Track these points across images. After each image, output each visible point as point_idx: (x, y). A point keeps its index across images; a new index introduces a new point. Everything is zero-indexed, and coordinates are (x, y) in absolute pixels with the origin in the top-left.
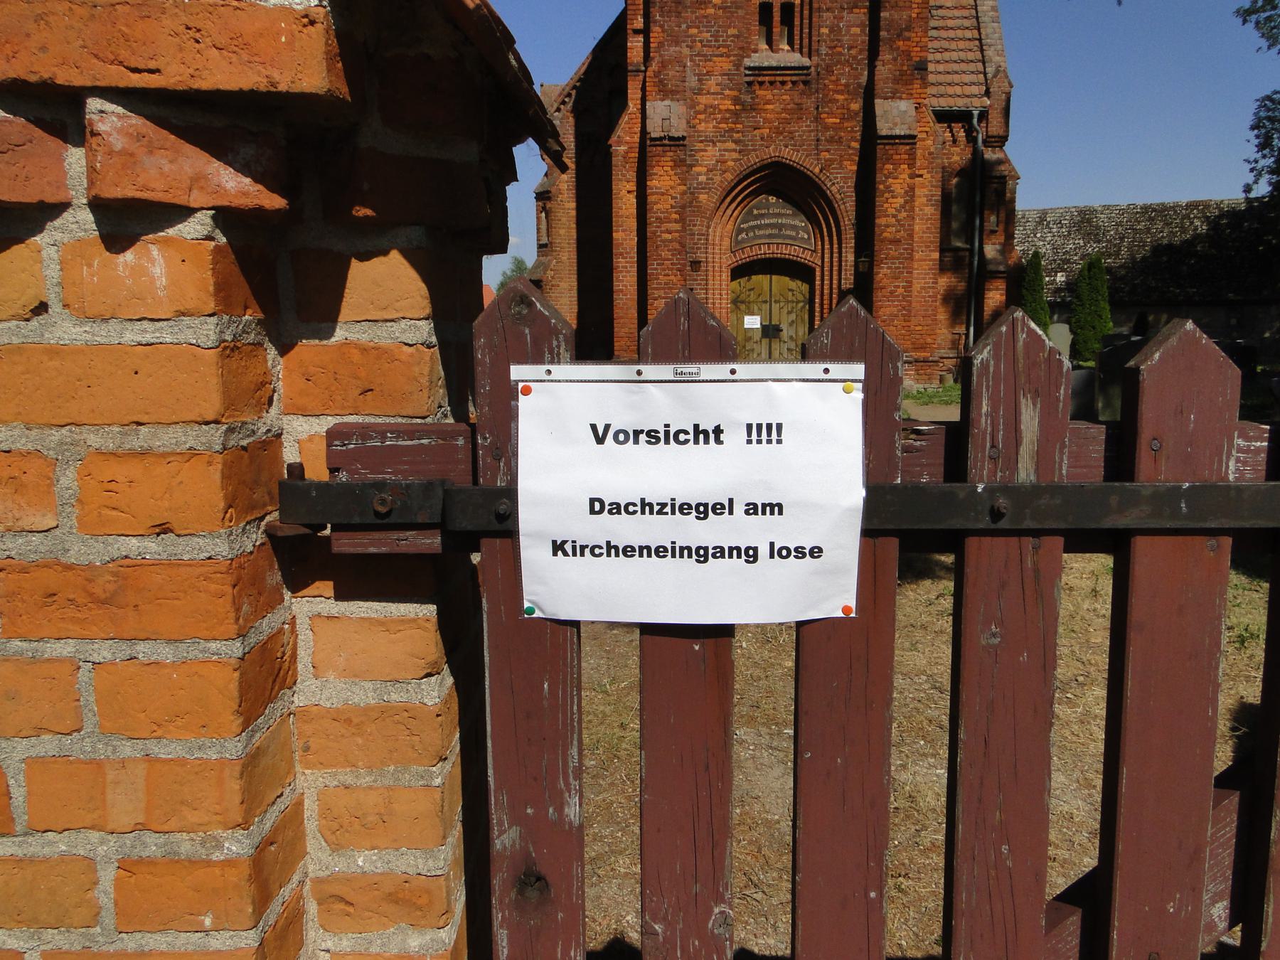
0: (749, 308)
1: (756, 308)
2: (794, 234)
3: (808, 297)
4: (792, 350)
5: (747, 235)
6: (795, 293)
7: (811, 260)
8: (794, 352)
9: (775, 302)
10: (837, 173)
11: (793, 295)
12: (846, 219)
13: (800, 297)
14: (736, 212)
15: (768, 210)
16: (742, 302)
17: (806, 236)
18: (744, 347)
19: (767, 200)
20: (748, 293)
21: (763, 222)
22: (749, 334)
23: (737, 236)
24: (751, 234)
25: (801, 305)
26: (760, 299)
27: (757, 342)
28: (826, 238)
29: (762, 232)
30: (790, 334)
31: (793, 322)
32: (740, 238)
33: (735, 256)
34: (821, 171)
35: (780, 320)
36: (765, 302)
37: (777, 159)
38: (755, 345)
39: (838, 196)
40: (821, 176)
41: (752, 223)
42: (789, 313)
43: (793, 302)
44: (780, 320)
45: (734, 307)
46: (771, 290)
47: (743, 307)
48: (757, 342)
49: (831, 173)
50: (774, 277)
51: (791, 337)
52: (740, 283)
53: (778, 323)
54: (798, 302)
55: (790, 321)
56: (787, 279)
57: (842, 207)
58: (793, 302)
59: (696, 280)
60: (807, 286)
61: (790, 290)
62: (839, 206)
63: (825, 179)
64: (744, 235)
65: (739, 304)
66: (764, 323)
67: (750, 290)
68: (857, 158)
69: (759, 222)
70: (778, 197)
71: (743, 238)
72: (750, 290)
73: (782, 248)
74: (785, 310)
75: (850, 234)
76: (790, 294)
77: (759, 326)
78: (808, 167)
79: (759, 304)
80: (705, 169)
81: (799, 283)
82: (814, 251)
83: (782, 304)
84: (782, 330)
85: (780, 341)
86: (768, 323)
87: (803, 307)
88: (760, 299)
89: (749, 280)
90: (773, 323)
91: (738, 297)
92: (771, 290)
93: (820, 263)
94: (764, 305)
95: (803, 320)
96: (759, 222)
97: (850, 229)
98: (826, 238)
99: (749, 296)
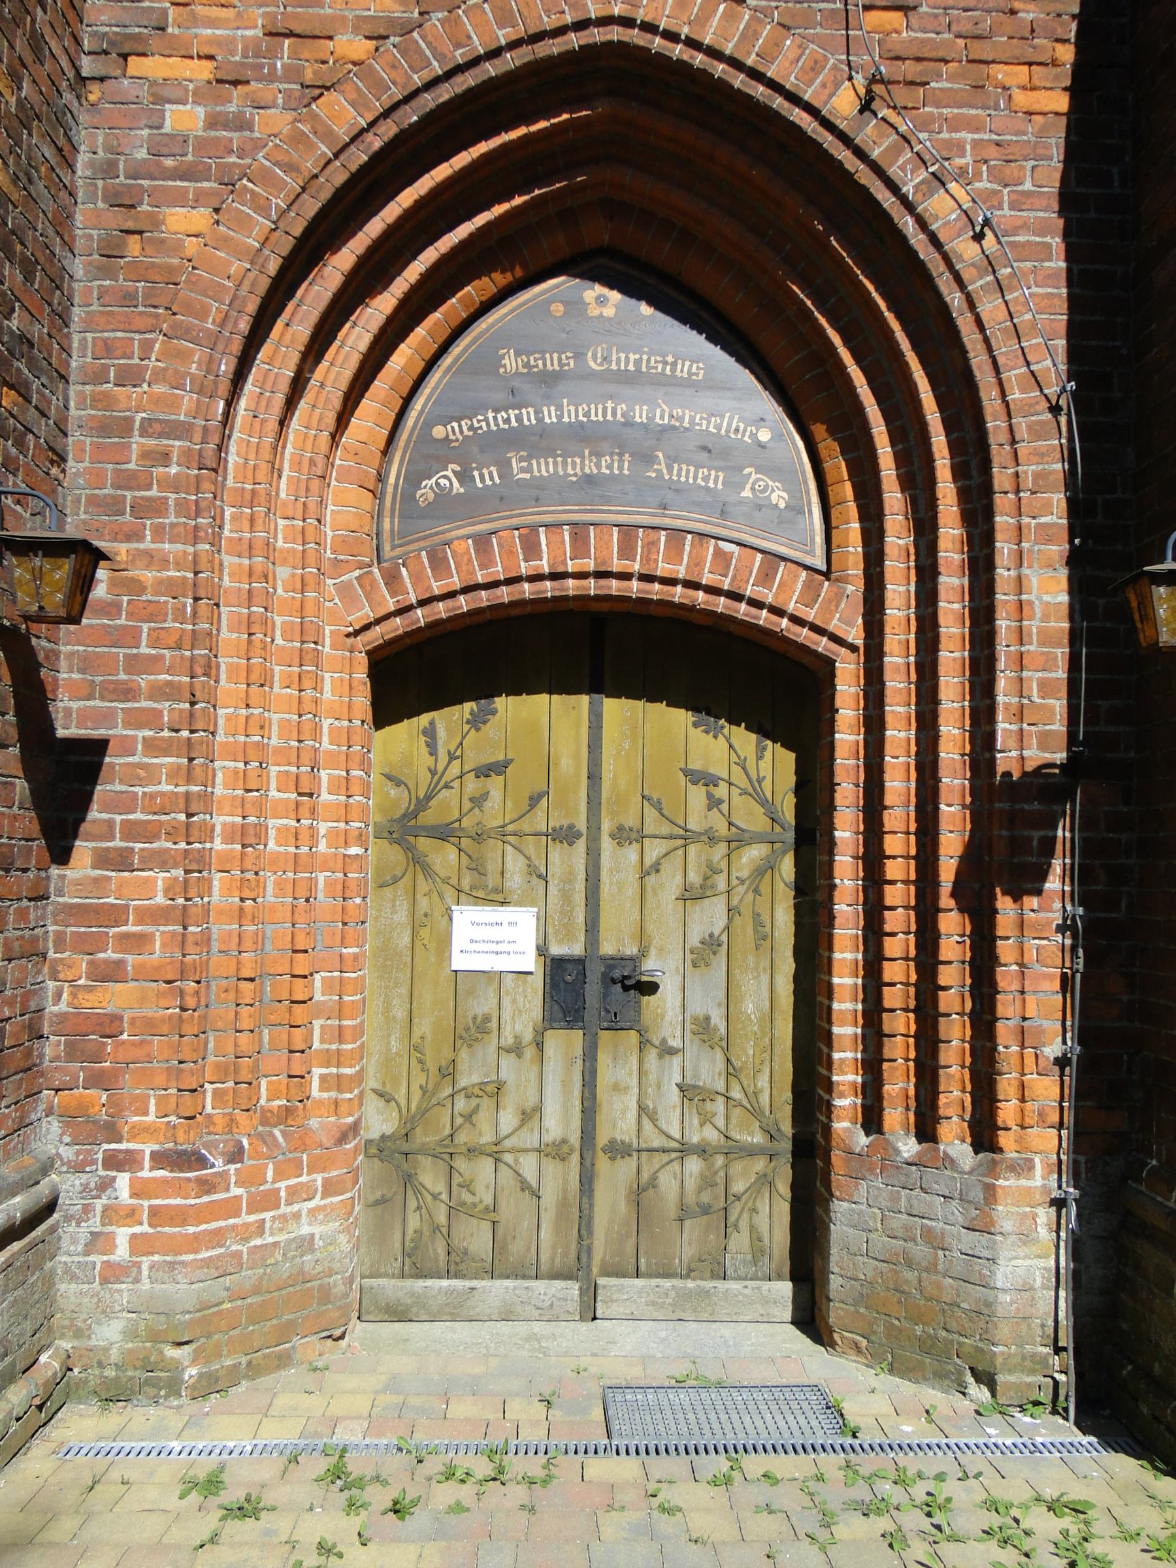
0: (478, 869)
1: (515, 864)
2: (715, 480)
3: (789, 816)
4: (706, 1095)
5: (464, 477)
6: (721, 791)
7: (810, 615)
8: (719, 1105)
9: (622, 836)
10: (955, 125)
11: (714, 803)
12: (1014, 374)
13: (752, 817)
14: (404, 358)
15: (579, 356)
16: (442, 833)
17: (779, 497)
18: (449, 1072)
19: (576, 307)
20: (472, 785)
21: (550, 416)
22: (483, 1005)
23: (414, 479)
24: (487, 477)
25: (754, 853)
26: (538, 820)
27: (516, 1049)
28: (894, 498)
29: (543, 468)
30: (697, 1008)
31: (711, 943)
32: (427, 490)
33: (392, 579)
34: (866, 107)
35: (642, 934)
36: (567, 836)
37: (615, 34)
38: (507, 1061)
39: (965, 250)
40: (869, 134)
41: (491, 421)
42: (690, 896)
43: (711, 838)
44: (642, 934)
45: (396, 855)
46: (594, 777)
47: (445, 858)
48: (516, 1049)
49: (925, 124)
50: (615, 709)
51: (703, 1027)
52: (430, 733)
53: (631, 950)
54: (738, 841)
55: (694, 940)
56: (681, 717)
57: (990, 308)
58: (711, 838)
59: (128, 693)
60: (788, 759)
61: (695, 777)
62: (971, 305)
63: (894, 152)
64: (447, 479)
65: (423, 843)
66: (556, 950)
67: (485, 771)
68: (1067, 54)
69: (529, 416)
70: (631, 290)
71: (442, 495)
72: (485, 771)
73: (651, 545)
74: (670, 883)
75: (1041, 455)
76: (697, 795)
77: (529, 961)
78: (790, 83)
79: (530, 845)
80: (203, 71)
81: (744, 739)
82: (827, 575)
83: (654, 850)
84: (650, 988)
85: (643, 1044)
86: (576, 949)
87: (768, 867)
88: (538, 820)
89: (477, 722)
90: (608, 948)
91: (422, 804)
92: (594, 777)
93: (855, 634)
94: (557, 853)
95: (764, 938)
96: (529, 416)
97: (1037, 432)
98: (894, 498)
99: (478, 801)
